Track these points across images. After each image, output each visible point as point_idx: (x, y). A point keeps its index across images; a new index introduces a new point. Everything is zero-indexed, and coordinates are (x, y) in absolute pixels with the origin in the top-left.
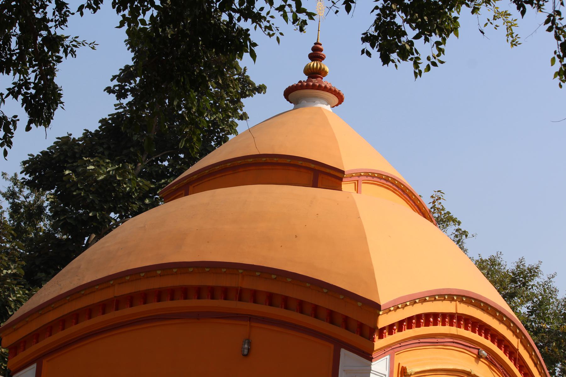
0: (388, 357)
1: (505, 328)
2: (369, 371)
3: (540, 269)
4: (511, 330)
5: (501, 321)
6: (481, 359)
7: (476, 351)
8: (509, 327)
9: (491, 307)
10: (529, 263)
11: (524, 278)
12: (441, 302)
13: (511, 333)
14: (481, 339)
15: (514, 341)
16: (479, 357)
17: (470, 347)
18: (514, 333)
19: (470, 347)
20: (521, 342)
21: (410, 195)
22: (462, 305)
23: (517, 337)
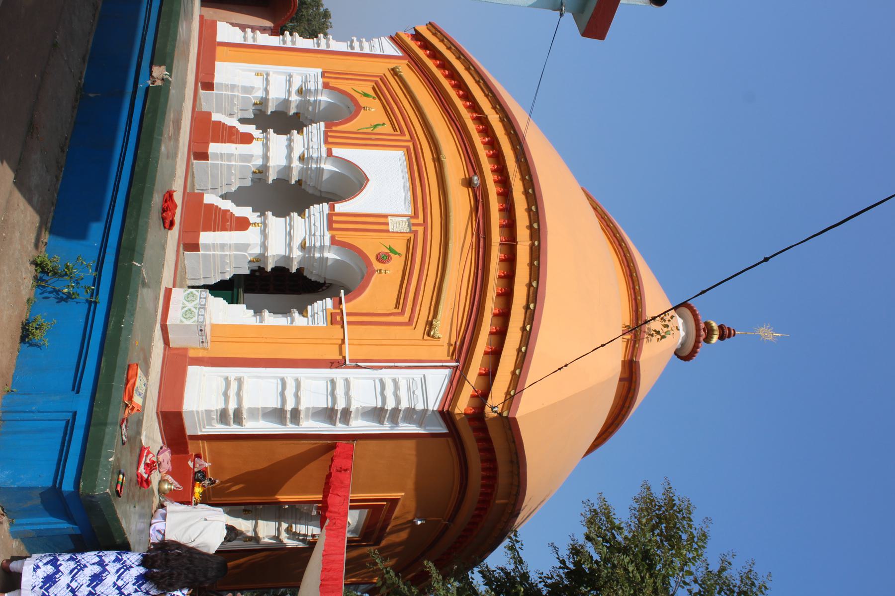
0: (401, 54)
1: (526, 206)
2: (378, 37)
16: (468, 183)
21: (636, 283)
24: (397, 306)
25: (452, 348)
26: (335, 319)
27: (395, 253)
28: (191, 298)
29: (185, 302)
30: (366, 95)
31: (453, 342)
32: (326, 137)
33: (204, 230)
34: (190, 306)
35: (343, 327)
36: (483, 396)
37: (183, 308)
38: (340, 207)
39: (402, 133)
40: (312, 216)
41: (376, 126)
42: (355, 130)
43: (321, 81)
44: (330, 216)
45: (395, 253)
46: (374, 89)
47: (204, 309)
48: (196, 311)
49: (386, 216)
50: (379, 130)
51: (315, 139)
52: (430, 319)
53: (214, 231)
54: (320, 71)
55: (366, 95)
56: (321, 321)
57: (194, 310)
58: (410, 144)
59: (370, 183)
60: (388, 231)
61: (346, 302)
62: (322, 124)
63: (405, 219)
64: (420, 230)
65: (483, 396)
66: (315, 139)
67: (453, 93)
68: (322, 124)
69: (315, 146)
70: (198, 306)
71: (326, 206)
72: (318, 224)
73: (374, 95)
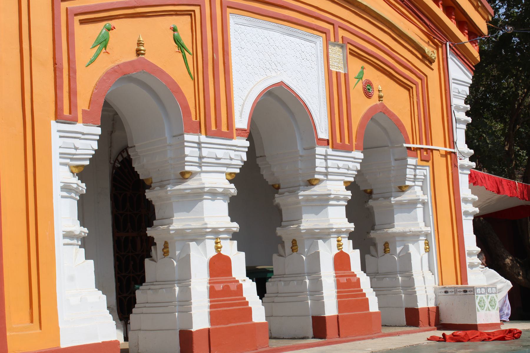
24: (408, 88)
25: (431, 43)
26: (426, 156)
27: (362, 73)
28: (483, 304)
29: (485, 308)
30: (103, 43)
31: (427, 39)
32: (219, 134)
33: (367, 308)
34: (487, 304)
35: (432, 150)
36: (473, 32)
37: (489, 310)
38: (323, 133)
40: (330, 170)
41: (177, 41)
42: (193, 82)
43: (79, 127)
44: (335, 148)
45: (362, 73)
46: (83, 22)
47: (488, 288)
48: (490, 295)
49: (329, 72)
50: (187, 41)
51: (220, 153)
52: (420, 57)
53: (338, 297)
54: (55, 126)
55: (103, 43)
56: (425, 172)
57: (489, 298)
59: (288, 82)
61: (409, 143)
62: (188, 137)
63: (330, 47)
64: (341, 33)
65: (473, 32)
66: (220, 153)
68: (188, 137)
69: (232, 154)
70: (487, 295)
71: (320, 150)
72: (341, 164)
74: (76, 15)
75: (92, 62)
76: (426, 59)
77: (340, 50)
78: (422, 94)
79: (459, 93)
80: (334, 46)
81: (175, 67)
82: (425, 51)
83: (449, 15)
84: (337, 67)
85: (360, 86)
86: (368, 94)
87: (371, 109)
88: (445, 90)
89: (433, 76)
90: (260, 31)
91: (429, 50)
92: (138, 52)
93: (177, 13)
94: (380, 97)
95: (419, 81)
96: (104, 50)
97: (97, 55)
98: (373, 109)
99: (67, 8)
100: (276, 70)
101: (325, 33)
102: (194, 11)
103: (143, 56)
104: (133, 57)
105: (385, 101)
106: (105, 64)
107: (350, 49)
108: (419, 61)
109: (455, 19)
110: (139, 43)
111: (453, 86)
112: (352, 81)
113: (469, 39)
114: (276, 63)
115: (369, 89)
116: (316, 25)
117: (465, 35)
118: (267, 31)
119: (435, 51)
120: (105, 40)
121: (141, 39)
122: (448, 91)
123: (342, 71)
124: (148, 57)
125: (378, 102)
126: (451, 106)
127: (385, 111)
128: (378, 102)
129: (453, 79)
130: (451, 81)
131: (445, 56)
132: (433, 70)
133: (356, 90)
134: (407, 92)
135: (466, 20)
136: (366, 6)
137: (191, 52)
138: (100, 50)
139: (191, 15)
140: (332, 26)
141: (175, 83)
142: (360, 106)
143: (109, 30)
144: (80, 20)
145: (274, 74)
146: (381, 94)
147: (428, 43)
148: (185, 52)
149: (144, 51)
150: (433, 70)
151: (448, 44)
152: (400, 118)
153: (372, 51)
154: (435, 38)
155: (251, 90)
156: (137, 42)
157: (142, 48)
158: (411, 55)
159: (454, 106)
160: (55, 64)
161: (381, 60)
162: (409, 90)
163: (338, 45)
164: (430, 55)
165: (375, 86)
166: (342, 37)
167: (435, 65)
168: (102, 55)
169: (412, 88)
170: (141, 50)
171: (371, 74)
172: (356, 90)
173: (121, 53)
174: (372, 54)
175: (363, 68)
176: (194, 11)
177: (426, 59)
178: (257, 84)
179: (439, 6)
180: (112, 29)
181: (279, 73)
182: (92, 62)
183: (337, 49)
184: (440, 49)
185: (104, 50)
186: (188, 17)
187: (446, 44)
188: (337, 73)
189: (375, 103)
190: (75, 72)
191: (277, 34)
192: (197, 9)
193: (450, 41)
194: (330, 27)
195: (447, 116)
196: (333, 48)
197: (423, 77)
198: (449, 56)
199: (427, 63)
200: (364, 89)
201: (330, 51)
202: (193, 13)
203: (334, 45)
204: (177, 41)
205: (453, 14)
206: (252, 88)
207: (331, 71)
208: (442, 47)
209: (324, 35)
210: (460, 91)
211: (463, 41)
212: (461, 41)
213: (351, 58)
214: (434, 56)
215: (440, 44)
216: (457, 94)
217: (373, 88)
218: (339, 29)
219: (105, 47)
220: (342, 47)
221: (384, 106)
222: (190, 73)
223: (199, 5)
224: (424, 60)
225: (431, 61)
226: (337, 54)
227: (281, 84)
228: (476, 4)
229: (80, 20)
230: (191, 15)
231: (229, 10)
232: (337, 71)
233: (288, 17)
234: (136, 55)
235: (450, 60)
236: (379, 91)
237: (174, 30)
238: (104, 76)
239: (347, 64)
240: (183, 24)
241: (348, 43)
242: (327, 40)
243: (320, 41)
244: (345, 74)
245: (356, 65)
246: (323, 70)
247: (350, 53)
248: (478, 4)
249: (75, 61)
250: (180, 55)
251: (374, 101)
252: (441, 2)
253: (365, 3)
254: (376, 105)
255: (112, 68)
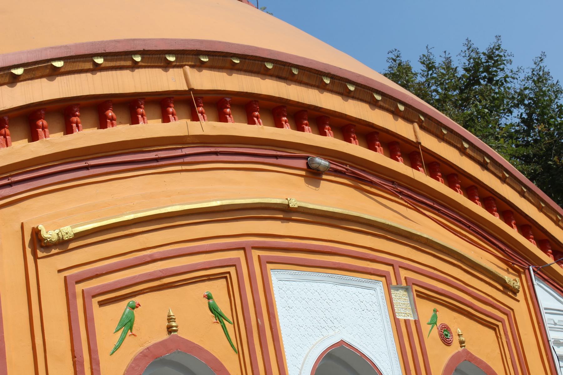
3: (502, 47)
4: (382, 108)
5: (346, 95)
6: (324, 177)
7: (302, 163)
8: (374, 104)
9: (297, 67)
10: (483, 47)
11: (487, 69)
12: (127, 72)
13: (389, 117)
14: (308, 137)
15: (405, 129)
17: (276, 157)
18: (396, 114)
19: (276, 157)
20: (421, 127)
22: (206, 73)
23: (411, 121)
24: (493, 327)
25: (510, 270)
27: (435, 317)
30: (127, 324)
31: (505, 267)
39: (234, 264)
41: (213, 309)
42: (237, 356)
45: (435, 317)
46: (102, 304)
49: (396, 322)
50: (224, 308)
52: (501, 288)
55: (127, 324)
58: (255, 254)
60: (417, 322)
63: (392, 291)
64: (403, 273)
67: (120, 132)
73: (125, 303)
74: (94, 296)
75: (117, 348)
76: (508, 289)
77: (406, 293)
78: (512, 332)
79: (555, 324)
80: (397, 290)
81: (214, 341)
82: (505, 281)
83: (527, 236)
84: (405, 313)
85: (435, 332)
86: (446, 340)
87: (453, 358)
88: (538, 323)
89: (520, 308)
90: (308, 284)
91: (510, 278)
92: (170, 329)
93: (210, 278)
94: (462, 342)
95: (505, 317)
96: (129, 333)
97: (122, 340)
98: (456, 358)
99: (83, 290)
100: (334, 328)
101: (385, 276)
102: (229, 273)
103: (176, 333)
104: (165, 336)
105: (468, 347)
106: (133, 348)
107: (416, 291)
108: (500, 293)
109: (534, 239)
110: (170, 319)
111: (547, 318)
112: (425, 328)
113: (555, 260)
114: (332, 319)
115: (447, 335)
116: (373, 269)
117: (549, 256)
118: (316, 284)
119: (518, 279)
120: (130, 321)
121: (172, 314)
122: (541, 324)
123: (411, 318)
124: (182, 333)
125: (460, 349)
126: (548, 341)
127: (470, 358)
128: (460, 349)
129: (546, 309)
130: (543, 311)
131: (530, 283)
132: (518, 301)
133: (432, 337)
134: (492, 332)
135: (547, 238)
136: (427, 239)
137: (232, 321)
138: (125, 333)
139: (226, 278)
140: (391, 267)
141: (217, 359)
142: (440, 357)
143: (133, 309)
144: (99, 302)
145: (331, 333)
146: (462, 338)
147: (507, 271)
148: (225, 322)
149: (176, 327)
150: (518, 301)
151: (531, 268)
152: (489, 364)
153: (443, 290)
154: (514, 264)
155: (307, 356)
156: (167, 318)
157: (174, 324)
158: (490, 288)
159: (552, 340)
160: (74, 357)
161: (456, 298)
162: (494, 329)
163: (402, 288)
164: (512, 284)
165: (453, 330)
166: (406, 278)
167: (520, 296)
168: (128, 339)
169: (498, 326)
170: (172, 327)
171: (446, 316)
172: (432, 337)
173: (150, 331)
174: (443, 293)
175: (435, 311)
176: (229, 273)
177: (508, 289)
178: (313, 347)
179: (512, 227)
180: (137, 307)
181: (337, 330)
182: (117, 348)
183: (401, 293)
184: (523, 276)
185: (129, 333)
186: (224, 281)
187: (529, 269)
188: (405, 321)
189: (457, 351)
190: (98, 364)
191: (329, 286)
192: (232, 270)
193: (533, 265)
194: (390, 269)
195: (547, 355)
196: (396, 292)
197: (509, 312)
198: (535, 282)
199: (511, 294)
200: (441, 335)
201: (393, 296)
202: (228, 275)
203: (397, 288)
204: (213, 309)
205: (531, 233)
206: (308, 354)
207: (398, 319)
208: (524, 273)
209: (384, 279)
210: (556, 322)
211: (549, 263)
212: (546, 263)
213: (419, 301)
214: (518, 284)
215: (521, 270)
216: (553, 326)
217: (451, 333)
218: (400, 269)
219: (131, 329)
220: (406, 289)
221: (468, 353)
222: (232, 346)
223: (235, 265)
224: (506, 291)
225: (515, 292)
226: (401, 298)
227: (342, 343)
228: (555, 218)
229: (99, 302)
230: (226, 278)
231: (269, 266)
232: (406, 318)
233: (339, 263)
234: (167, 333)
235: (537, 287)
236: (459, 335)
237: (209, 297)
238: (132, 363)
239: (416, 308)
240: (217, 289)
241: (414, 284)
242: (388, 284)
243: (380, 286)
244: (415, 321)
245: (426, 309)
246: (389, 320)
247: (418, 296)
248: (557, 218)
249: (97, 351)
250: (219, 326)
251: (455, 348)
252: (513, 222)
253: (425, 236)
254: (459, 352)
255: (141, 353)
